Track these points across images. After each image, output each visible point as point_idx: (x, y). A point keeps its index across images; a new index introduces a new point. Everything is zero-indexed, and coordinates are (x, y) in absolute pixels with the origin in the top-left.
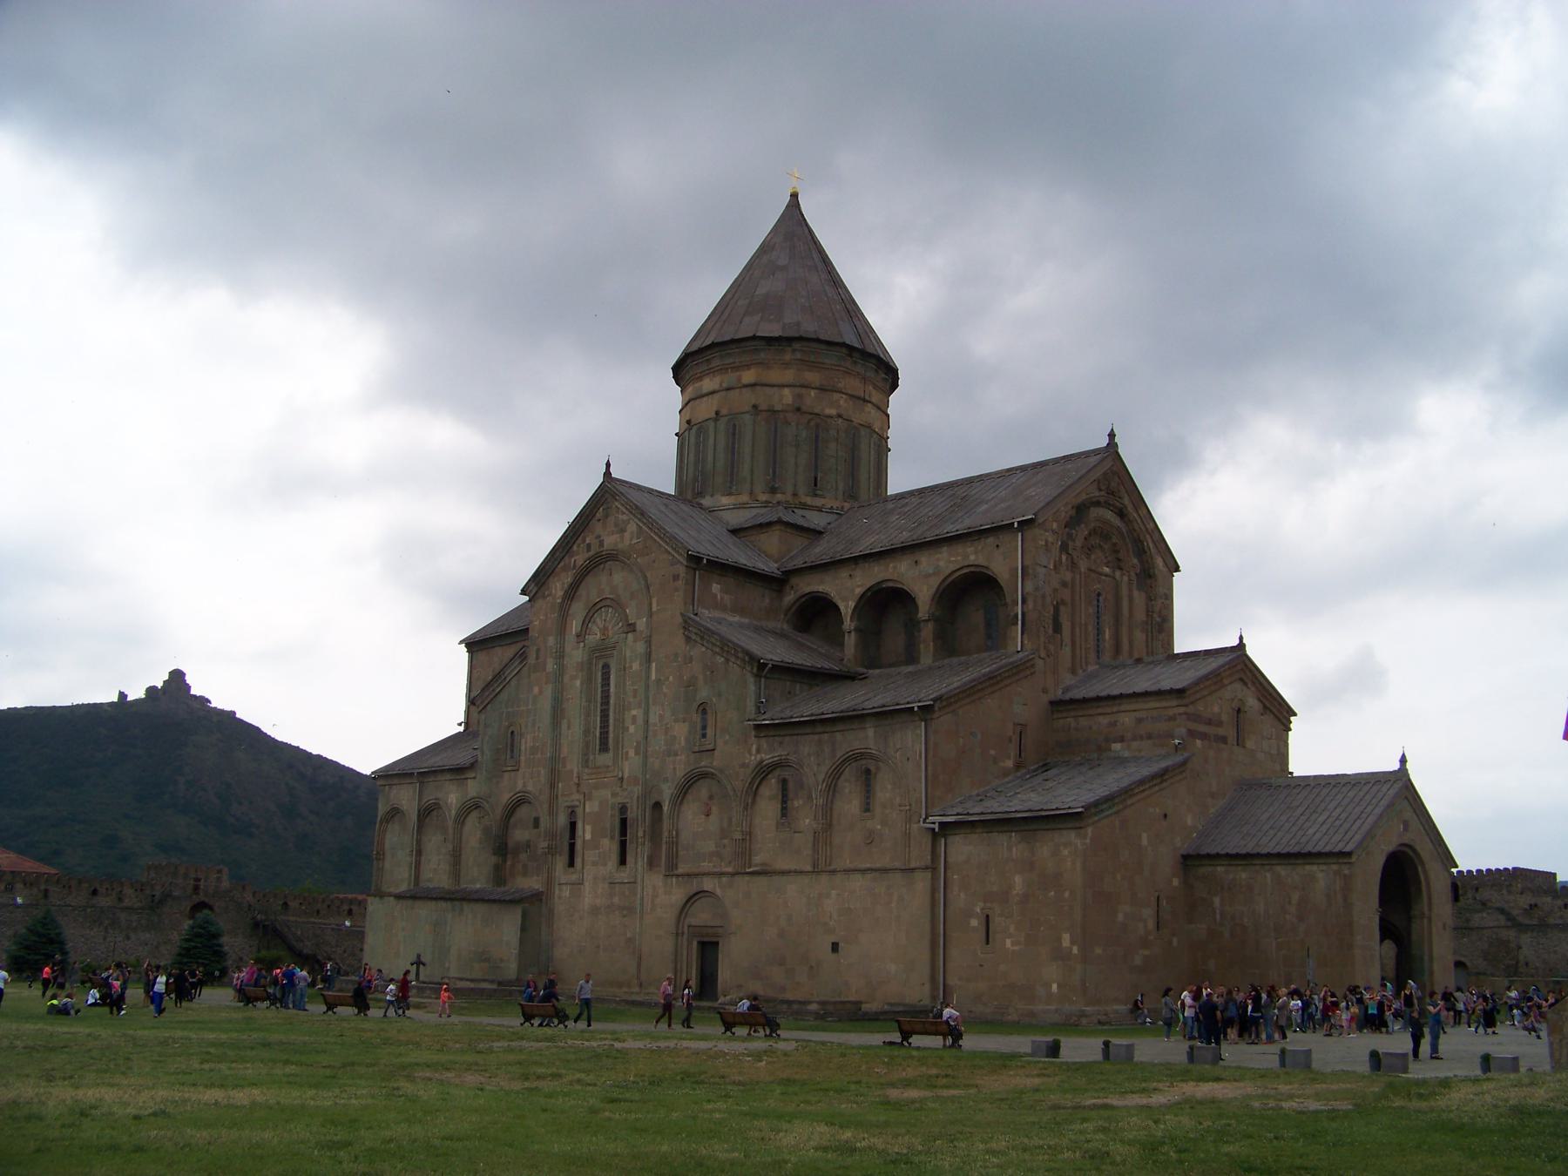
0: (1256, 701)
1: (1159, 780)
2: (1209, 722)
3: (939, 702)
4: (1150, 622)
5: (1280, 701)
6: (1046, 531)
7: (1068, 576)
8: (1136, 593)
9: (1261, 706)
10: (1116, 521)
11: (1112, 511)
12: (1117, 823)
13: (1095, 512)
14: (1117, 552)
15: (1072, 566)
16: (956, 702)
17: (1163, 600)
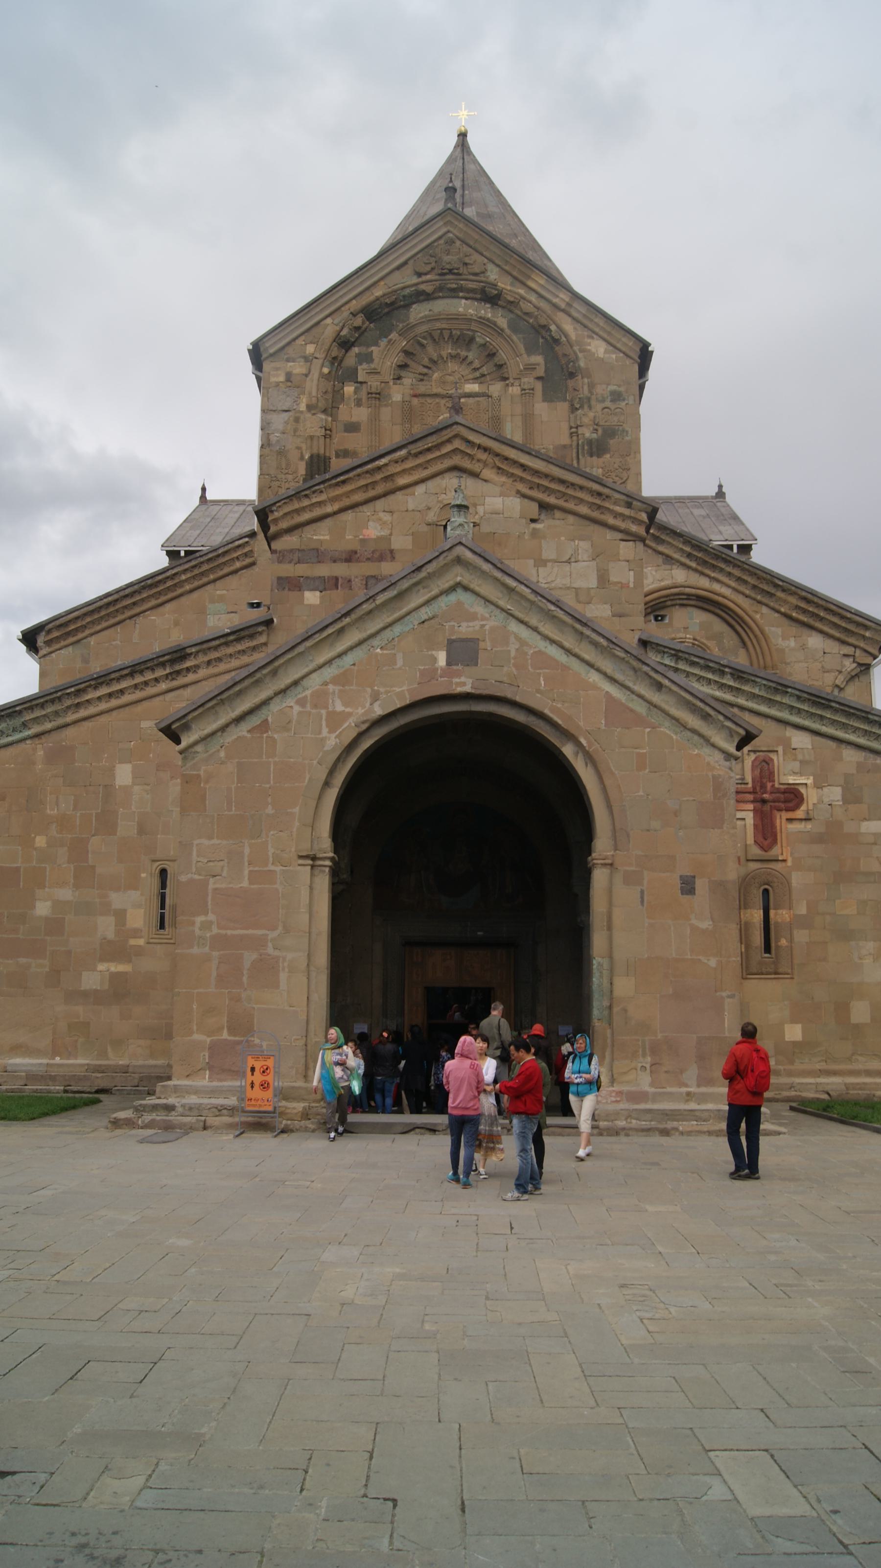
0: (515, 505)
1: (160, 672)
2: (350, 557)
3: (44, 633)
4: (575, 443)
5: (596, 487)
6: (288, 360)
7: (361, 414)
8: (541, 408)
9: (535, 506)
10: (486, 311)
11: (466, 299)
12: (40, 753)
13: (418, 312)
14: (492, 355)
15: (368, 398)
16: (84, 627)
17: (608, 404)
